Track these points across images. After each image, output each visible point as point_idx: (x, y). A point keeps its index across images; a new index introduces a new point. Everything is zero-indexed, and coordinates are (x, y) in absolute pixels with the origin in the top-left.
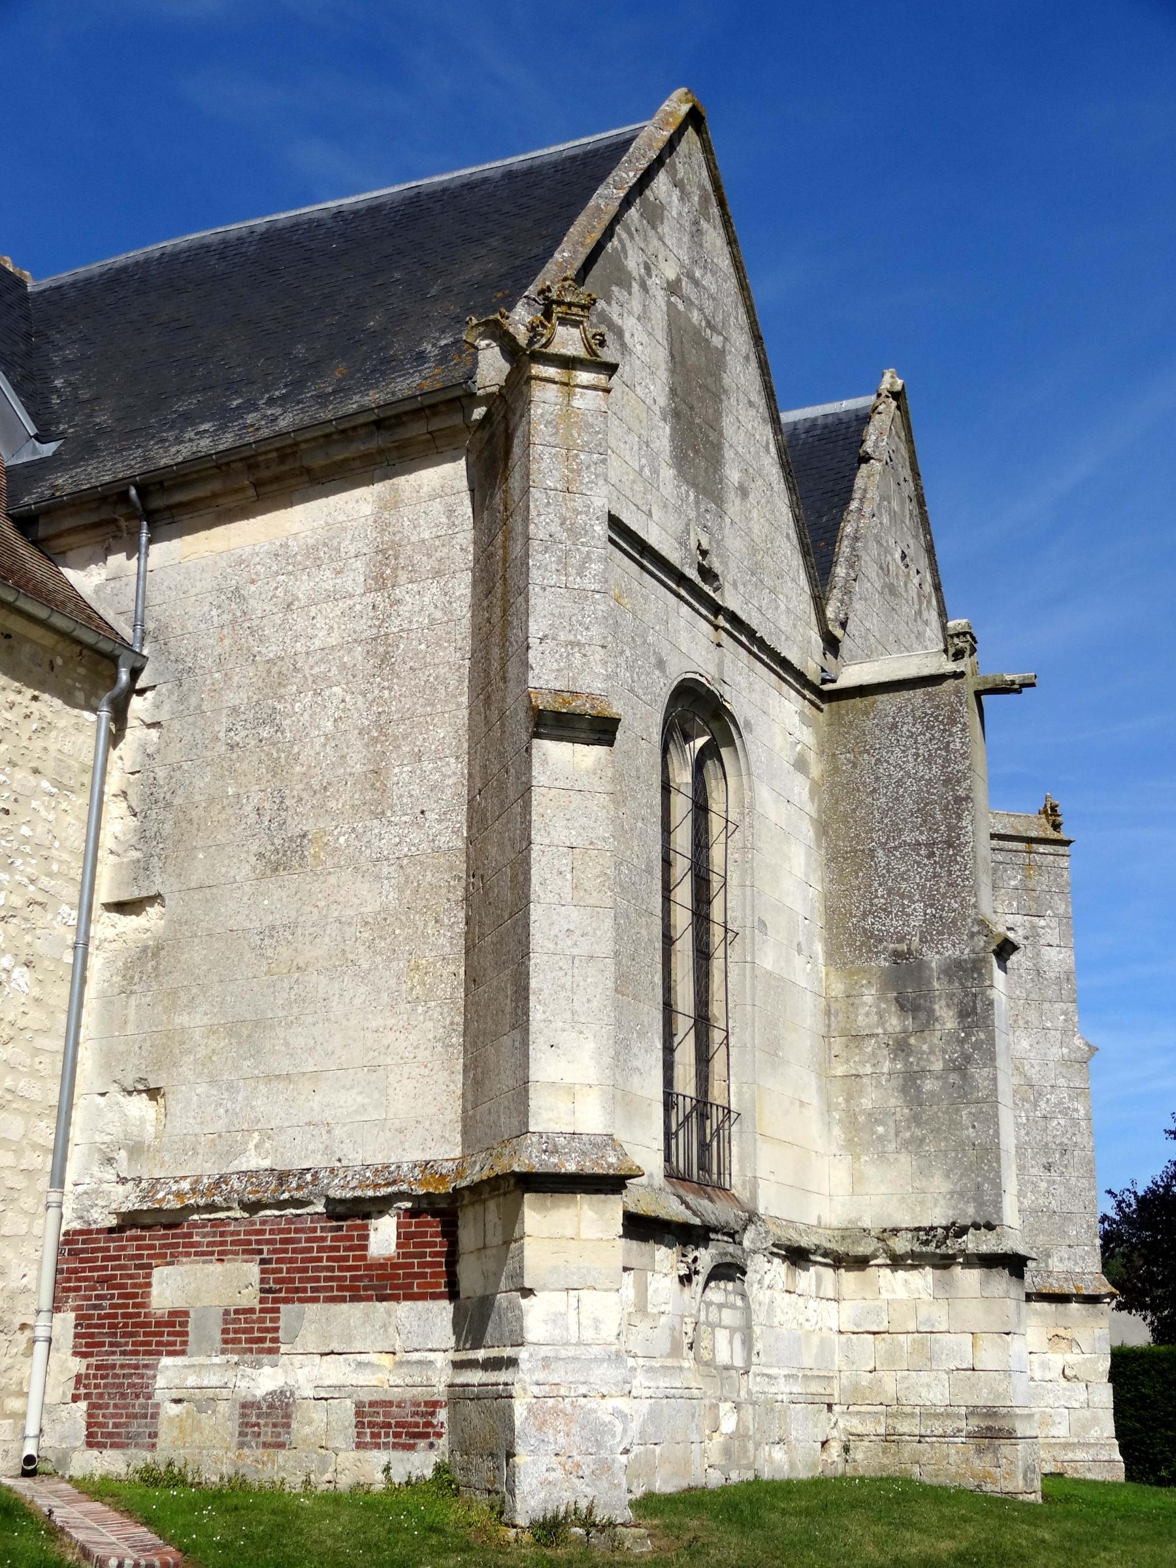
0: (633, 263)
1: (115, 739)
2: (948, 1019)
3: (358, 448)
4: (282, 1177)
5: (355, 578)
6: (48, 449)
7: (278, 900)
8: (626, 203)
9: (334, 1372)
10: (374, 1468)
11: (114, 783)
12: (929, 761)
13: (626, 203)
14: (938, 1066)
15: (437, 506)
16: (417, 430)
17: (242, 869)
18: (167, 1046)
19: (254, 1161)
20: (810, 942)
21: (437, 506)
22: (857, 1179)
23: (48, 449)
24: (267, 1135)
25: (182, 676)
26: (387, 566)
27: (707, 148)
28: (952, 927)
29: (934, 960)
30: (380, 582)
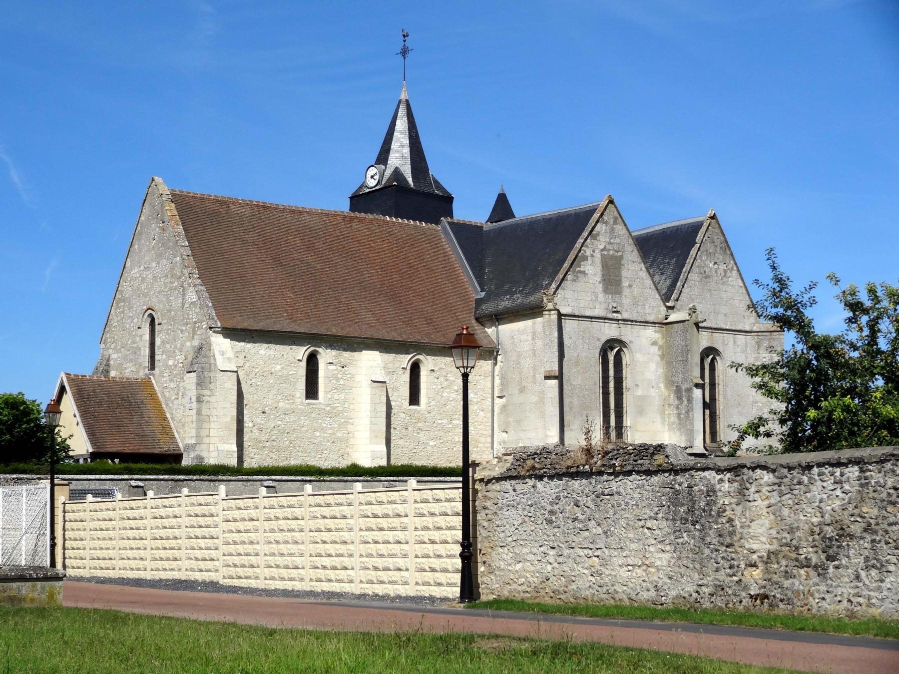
0: (588, 252)
1: (496, 364)
2: (686, 402)
5: (530, 338)
6: (483, 294)
8: (582, 246)
11: (496, 373)
13: (582, 246)
16: (536, 310)
17: (517, 392)
18: (507, 424)
20: (658, 384)
22: (670, 437)
23: (483, 294)
25: (505, 353)
27: (616, 207)
28: (686, 380)
29: (683, 388)
30: (533, 339)
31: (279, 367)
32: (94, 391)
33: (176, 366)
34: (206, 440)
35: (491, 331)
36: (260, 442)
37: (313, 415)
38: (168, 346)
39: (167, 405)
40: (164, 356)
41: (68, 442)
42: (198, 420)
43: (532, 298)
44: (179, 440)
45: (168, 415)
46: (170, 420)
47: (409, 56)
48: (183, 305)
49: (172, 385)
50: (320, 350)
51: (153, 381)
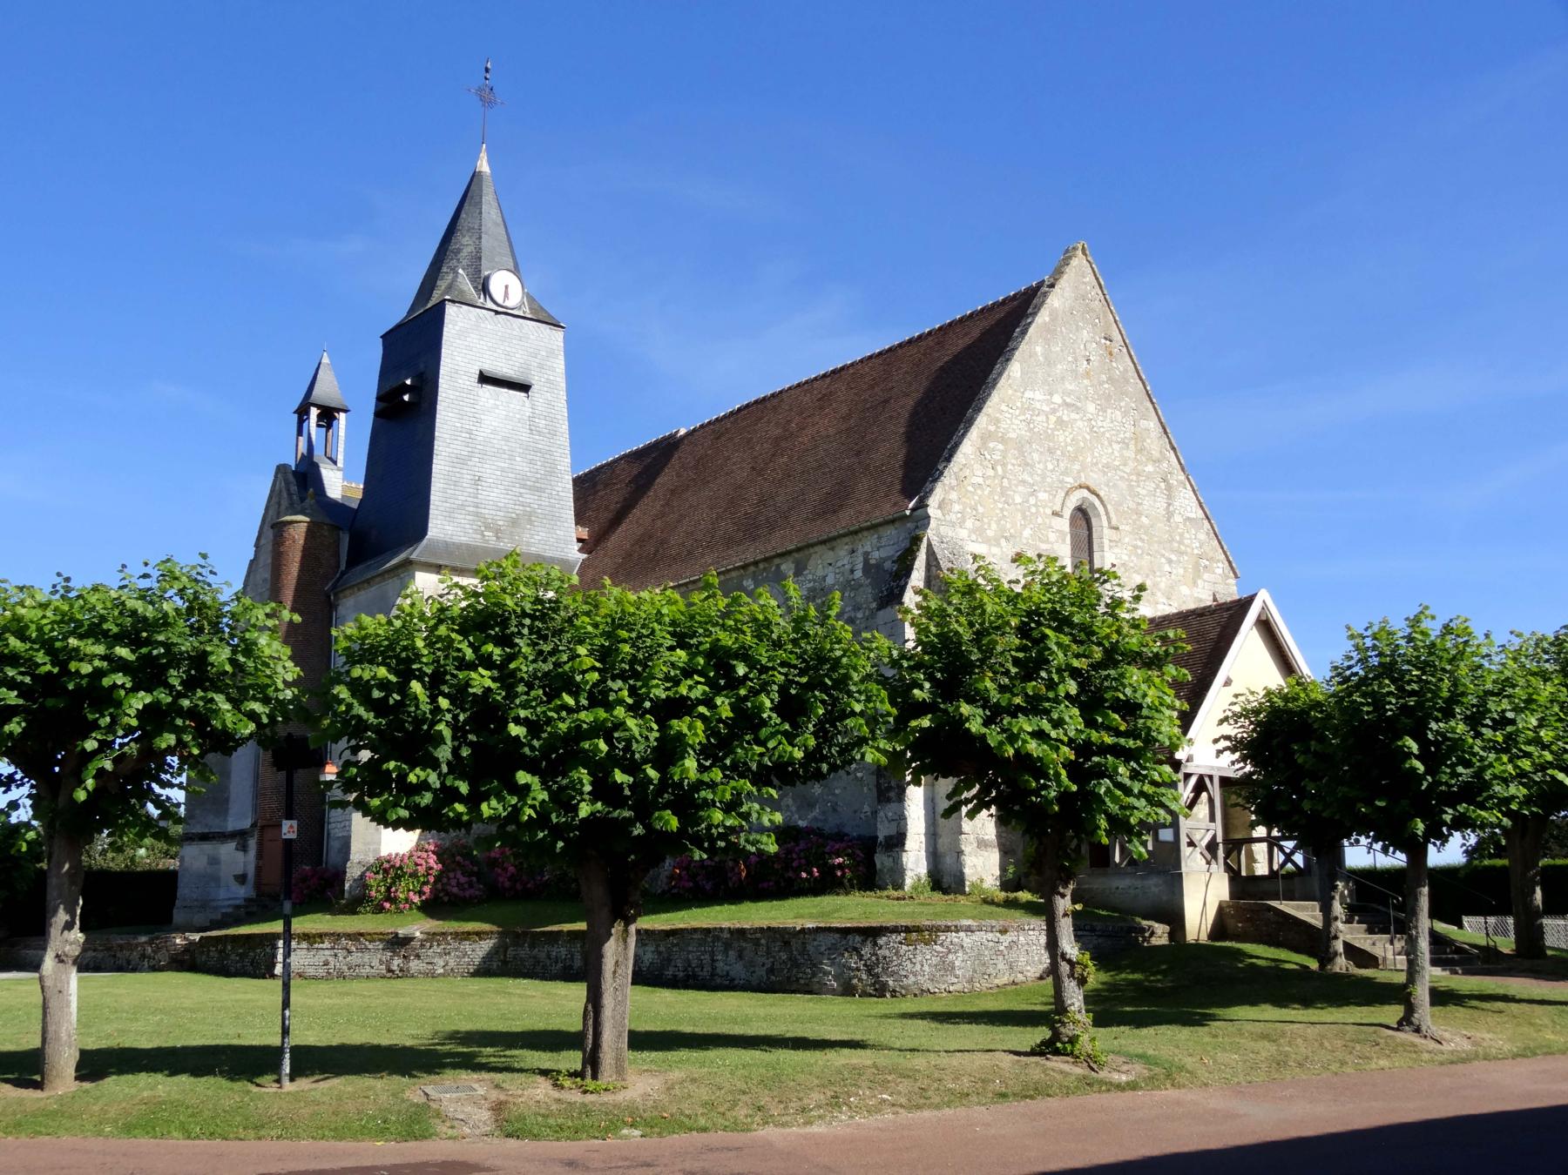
48: (1169, 515)
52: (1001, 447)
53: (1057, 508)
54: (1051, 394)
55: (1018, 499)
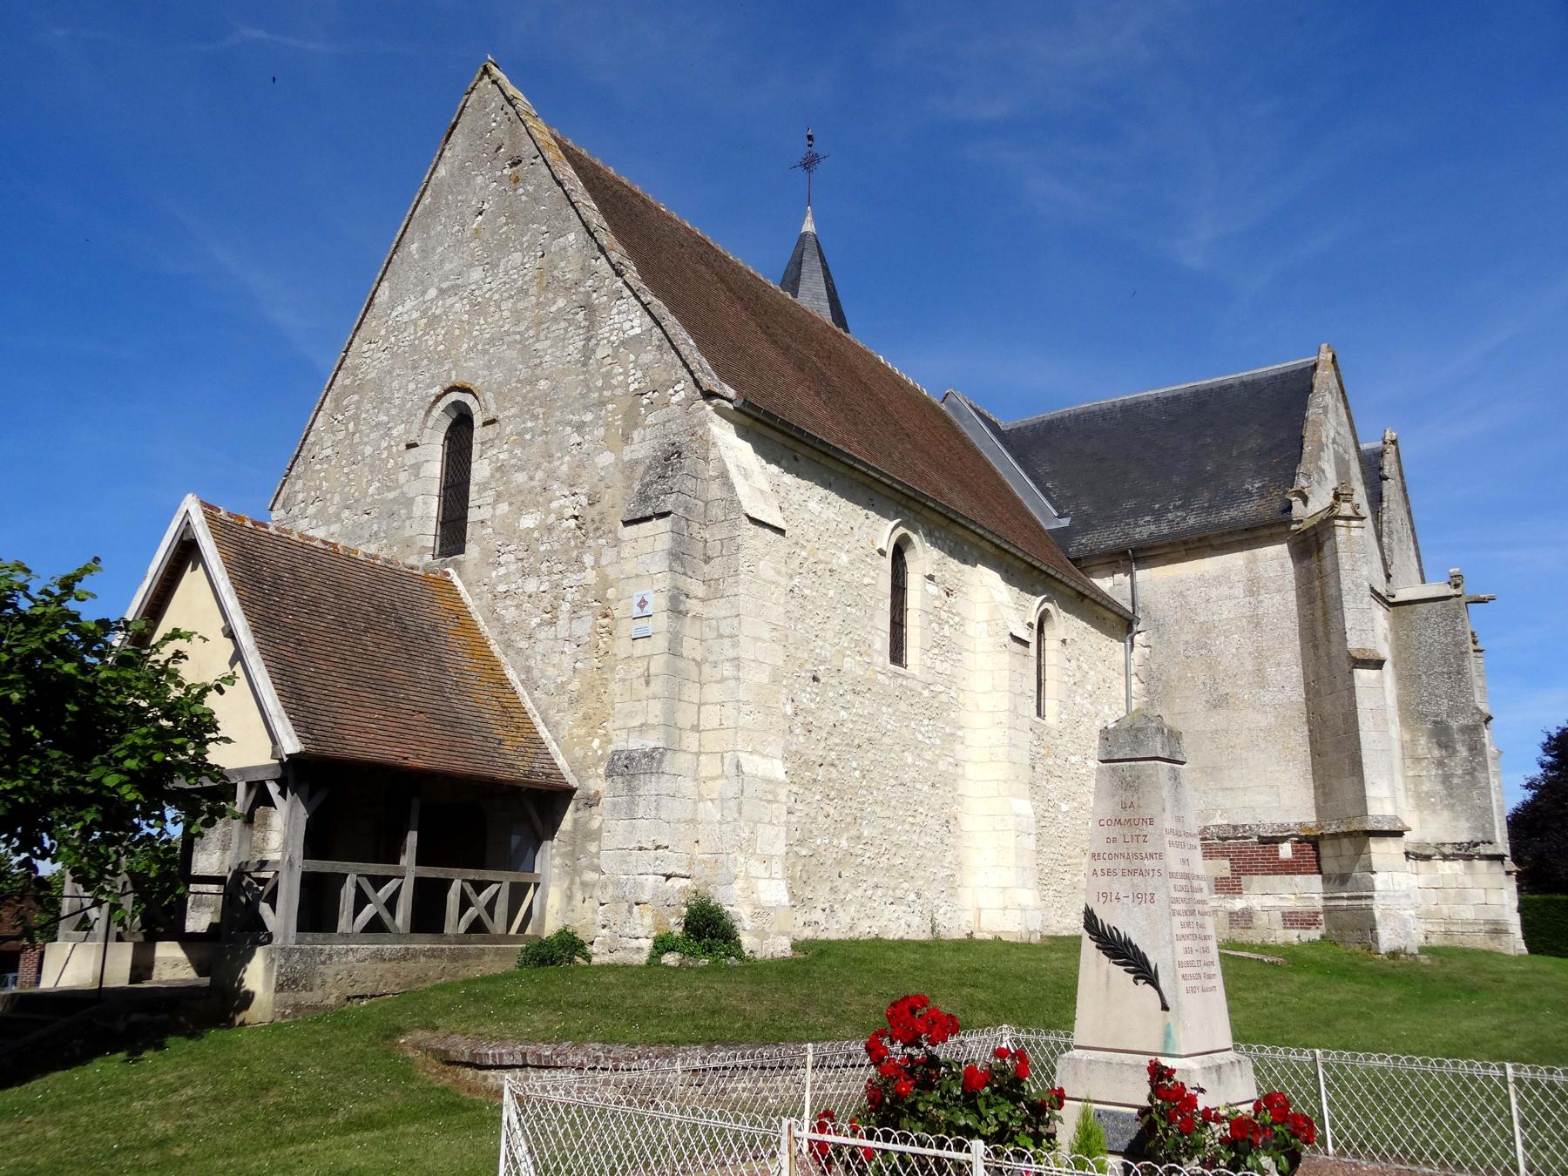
2: (1463, 752)
3: (1236, 538)
4: (1235, 828)
5: (1239, 590)
6: (1065, 522)
7: (1218, 719)
9: (1269, 901)
10: (1293, 936)
12: (1446, 635)
14: (1459, 772)
15: (1275, 563)
19: (1219, 821)
21: (1275, 563)
23: (1065, 522)
24: (1225, 811)
26: (1254, 586)
28: (1462, 711)
29: (1454, 725)
31: (845, 558)
32: (293, 570)
33: (550, 529)
34: (691, 741)
35: (1105, 584)
36: (807, 764)
37: (903, 706)
38: (520, 477)
39: (508, 645)
40: (503, 507)
41: (212, 701)
42: (673, 673)
43: (1234, 513)
44: (553, 748)
45: (511, 674)
46: (520, 689)
47: (821, 168)
48: (587, 353)
49: (531, 585)
50: (914, 538)
51: (457, 582)
52: (356, 397)
53: (412, 438)
54: (424, 293)
55: (368, 450)
